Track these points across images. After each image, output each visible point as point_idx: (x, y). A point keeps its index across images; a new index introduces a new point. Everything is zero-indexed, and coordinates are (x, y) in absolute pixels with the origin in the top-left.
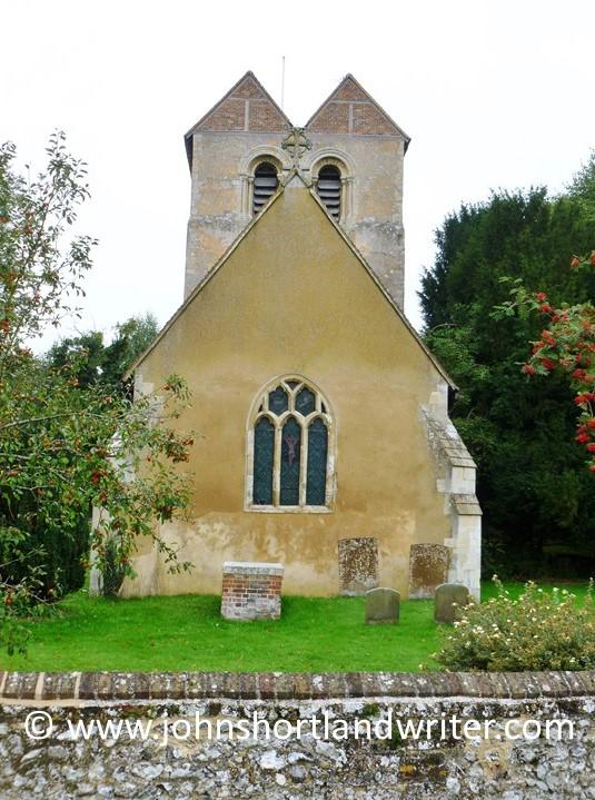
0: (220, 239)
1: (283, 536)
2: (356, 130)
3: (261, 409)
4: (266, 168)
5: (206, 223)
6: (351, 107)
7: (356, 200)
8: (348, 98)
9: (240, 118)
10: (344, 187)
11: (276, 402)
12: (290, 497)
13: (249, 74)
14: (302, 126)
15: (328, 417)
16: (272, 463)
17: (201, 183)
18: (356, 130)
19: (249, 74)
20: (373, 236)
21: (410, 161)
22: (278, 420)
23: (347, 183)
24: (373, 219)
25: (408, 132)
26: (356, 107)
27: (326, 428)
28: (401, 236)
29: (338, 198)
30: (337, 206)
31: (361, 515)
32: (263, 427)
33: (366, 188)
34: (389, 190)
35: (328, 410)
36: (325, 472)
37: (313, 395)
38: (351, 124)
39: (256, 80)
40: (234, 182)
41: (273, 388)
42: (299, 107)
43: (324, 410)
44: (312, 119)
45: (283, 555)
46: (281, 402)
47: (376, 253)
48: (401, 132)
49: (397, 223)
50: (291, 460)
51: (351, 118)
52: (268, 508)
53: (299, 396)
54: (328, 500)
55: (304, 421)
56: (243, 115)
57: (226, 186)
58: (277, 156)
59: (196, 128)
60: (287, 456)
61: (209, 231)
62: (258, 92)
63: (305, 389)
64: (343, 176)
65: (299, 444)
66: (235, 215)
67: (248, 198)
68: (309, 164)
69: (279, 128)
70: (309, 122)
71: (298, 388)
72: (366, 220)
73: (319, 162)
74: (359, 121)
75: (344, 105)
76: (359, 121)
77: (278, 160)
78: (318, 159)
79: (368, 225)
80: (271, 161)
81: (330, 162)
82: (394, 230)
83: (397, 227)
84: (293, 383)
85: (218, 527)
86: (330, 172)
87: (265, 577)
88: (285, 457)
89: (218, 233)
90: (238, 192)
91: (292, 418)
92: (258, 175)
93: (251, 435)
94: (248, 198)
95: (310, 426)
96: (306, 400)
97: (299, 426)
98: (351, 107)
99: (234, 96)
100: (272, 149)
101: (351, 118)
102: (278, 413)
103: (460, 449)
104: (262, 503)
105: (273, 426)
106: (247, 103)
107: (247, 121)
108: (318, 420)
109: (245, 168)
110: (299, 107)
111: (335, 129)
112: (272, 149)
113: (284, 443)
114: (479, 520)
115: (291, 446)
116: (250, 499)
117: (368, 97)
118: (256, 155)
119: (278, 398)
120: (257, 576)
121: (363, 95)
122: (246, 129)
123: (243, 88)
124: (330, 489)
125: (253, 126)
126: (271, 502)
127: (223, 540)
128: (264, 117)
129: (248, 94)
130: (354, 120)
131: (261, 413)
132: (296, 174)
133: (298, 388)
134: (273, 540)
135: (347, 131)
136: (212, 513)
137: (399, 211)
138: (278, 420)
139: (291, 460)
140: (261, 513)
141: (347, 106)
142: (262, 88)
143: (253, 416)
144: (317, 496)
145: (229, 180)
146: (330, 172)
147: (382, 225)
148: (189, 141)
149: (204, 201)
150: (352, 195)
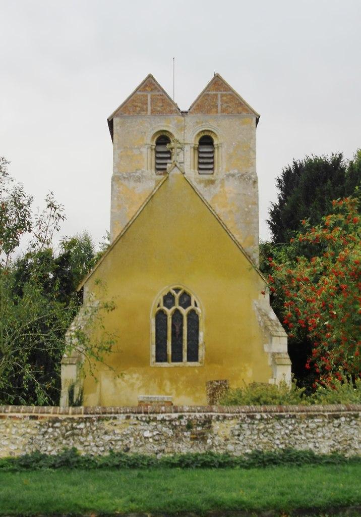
0: (134, 188)
1: (174, 380)
2: (223, 111)
3: (159, 306)
4: (163, 139)
5: (124, 178)
6: (219, 96)
8: (217, 90)
9: (145, 106)
10: (216, 150)
11: (168, 301)
12: (177, 357)
13: (150, 76)
14: (186, 109)
15: (198, 310)
16: (166, 338)
18: (223, 111)
19: (150, 76)
21: (261, 132)
22: (169, 312)
23: (218, 148)
24: (236, 171)
25: (258, 110)
26: (222, 96)
27: (197, 316)
28: (255, 182)
29: (213, 158)
30: (212, 169)
31: (219, 367)
32: (160, 317)
33: (231, 151)
34: (247, 152)
35: (198, 304)
36: (197, 341)
37: (189, 297)
39: (154, 80)
40: (142, 149)
41: (166, 293)
42: (184, 99)
43: (196, 305)
44: (193, 105)
45: (174, 391)
46: (171, 301)
47: (240, 194)
48: (253, 112)
49: (253, 173)
50: (177, 336)
51: (219, 103)
52: (165, 364)
53: (181, 297)
54: (200, 359)
55: (184, 312)
56: (147, 104)
57: (136, 152)
58: (171, 131)
59: (116, 114)
60: (175, 333)
61: (126, 183)
62: (156, 88)
63: (185, 293)
64: (215, 143)
65: (182, 325)
66: (143, 172)
67: (151, 159)
69: (171, 112)
70: (191, 107)
71: (180, 293)
72: (232, 172)
73: (198, 134)
74: (225, 105)
75: (215, 95)
76: (225, 105)
78: (198, 132)
79: (233, 175)
81: (206, 134)
84: (177, 290)
85: (135, 376)
86: (206, 140)
87: (162, 402)
88: (174, 334)
89: (132, 184)
90: (145, 156)
91: (177, 311)
92: (158, 144)
93: (153, 321)
94: (151, 159)
95: (188, 315)
96: (185, 299)
97: (181, 315)
98: (219, 96)
99: (140, 91)
101: (219, 103)
102: (169, 308)
103: (277, 325)
104: (161, 361)
105: (166, 316)
107: (149, 108)
109: (149, 141)
110: (184, 99)
111: (209, 111)
113: (173, 326)
114: (290, 368)
115: (177, 328)
116: (153, 359)
117: (230, 89)
119: (168, 299)
120: (158, 402)
121: (227, 88)
123: (146, 86)
124: (201, 352)
125: (152, 112)
126: (166, 360)
127: (138, 384)
128: (161, 104)
130: (221, 105)
131: (159, 308)
132: (176, 166)
133: (180, 293)
134: (168, 383)
136: (131, 368)
137: (253, 165)
138: (169, 312)
139: (177, 336)
140: (161, 367)
141: (216, 95)
142: (159, 86)
143: (153, 311)
144: (193, 356)
145: (139, 148)
146: (206, 140)
147: (243, 175)
148: (111, 123)
150: (221, 156)
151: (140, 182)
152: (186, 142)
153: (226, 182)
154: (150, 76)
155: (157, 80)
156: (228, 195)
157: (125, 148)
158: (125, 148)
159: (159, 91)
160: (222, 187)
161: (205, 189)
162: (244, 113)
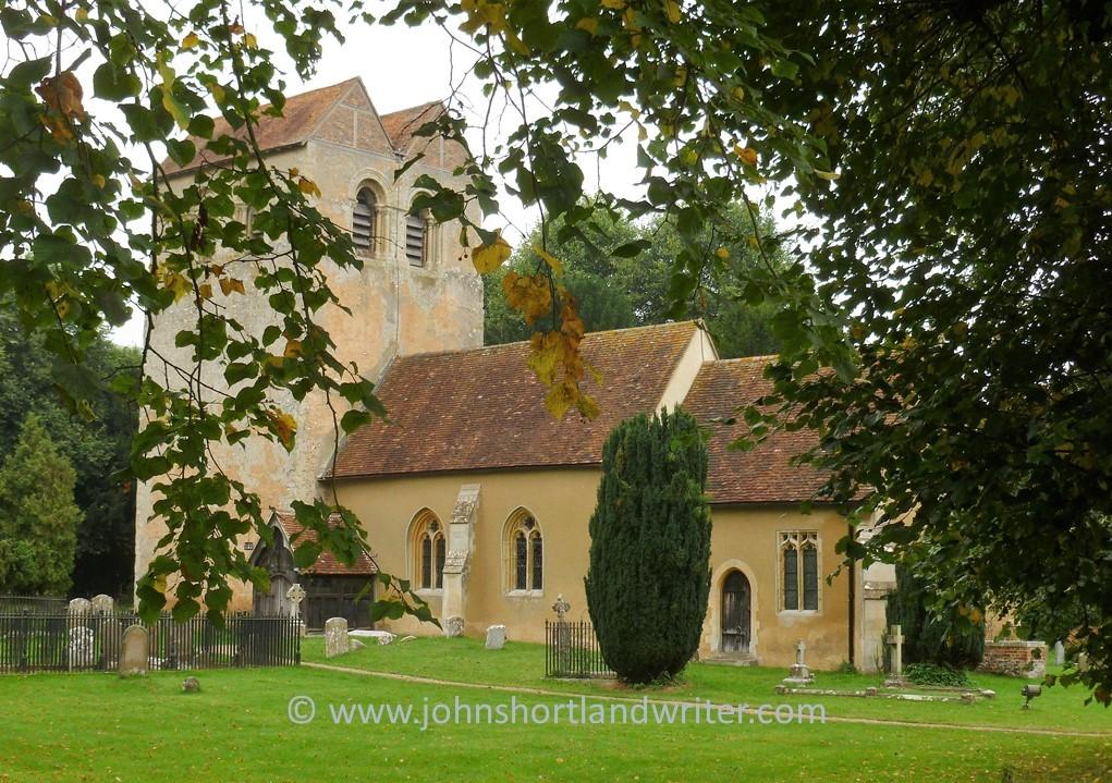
19: (358, 80)
20: (461, 289)
24: (459, 270)
47: (463, 308)
51: (442, 152)
56: (352, 127)
58: (381, 183)
74: (448, 155)
77: (381, 187)
79: (456, 276)
80: (372, 187)
100: (377, 174)
106: (356, 114)
112: (377, 174)
118: (362, 179)
122: (355, 143)
125: (361, 143)
128: (370, 134)
129: (356, 103)
135: (439, 166)
145: (339, 204)
147: (466, 277)
152: (400, 207)
154: (358, 80)
155: (368, 89)
156: (450, 308)
159: (368, 109)
160: (444, 292)
161: (423, 292)
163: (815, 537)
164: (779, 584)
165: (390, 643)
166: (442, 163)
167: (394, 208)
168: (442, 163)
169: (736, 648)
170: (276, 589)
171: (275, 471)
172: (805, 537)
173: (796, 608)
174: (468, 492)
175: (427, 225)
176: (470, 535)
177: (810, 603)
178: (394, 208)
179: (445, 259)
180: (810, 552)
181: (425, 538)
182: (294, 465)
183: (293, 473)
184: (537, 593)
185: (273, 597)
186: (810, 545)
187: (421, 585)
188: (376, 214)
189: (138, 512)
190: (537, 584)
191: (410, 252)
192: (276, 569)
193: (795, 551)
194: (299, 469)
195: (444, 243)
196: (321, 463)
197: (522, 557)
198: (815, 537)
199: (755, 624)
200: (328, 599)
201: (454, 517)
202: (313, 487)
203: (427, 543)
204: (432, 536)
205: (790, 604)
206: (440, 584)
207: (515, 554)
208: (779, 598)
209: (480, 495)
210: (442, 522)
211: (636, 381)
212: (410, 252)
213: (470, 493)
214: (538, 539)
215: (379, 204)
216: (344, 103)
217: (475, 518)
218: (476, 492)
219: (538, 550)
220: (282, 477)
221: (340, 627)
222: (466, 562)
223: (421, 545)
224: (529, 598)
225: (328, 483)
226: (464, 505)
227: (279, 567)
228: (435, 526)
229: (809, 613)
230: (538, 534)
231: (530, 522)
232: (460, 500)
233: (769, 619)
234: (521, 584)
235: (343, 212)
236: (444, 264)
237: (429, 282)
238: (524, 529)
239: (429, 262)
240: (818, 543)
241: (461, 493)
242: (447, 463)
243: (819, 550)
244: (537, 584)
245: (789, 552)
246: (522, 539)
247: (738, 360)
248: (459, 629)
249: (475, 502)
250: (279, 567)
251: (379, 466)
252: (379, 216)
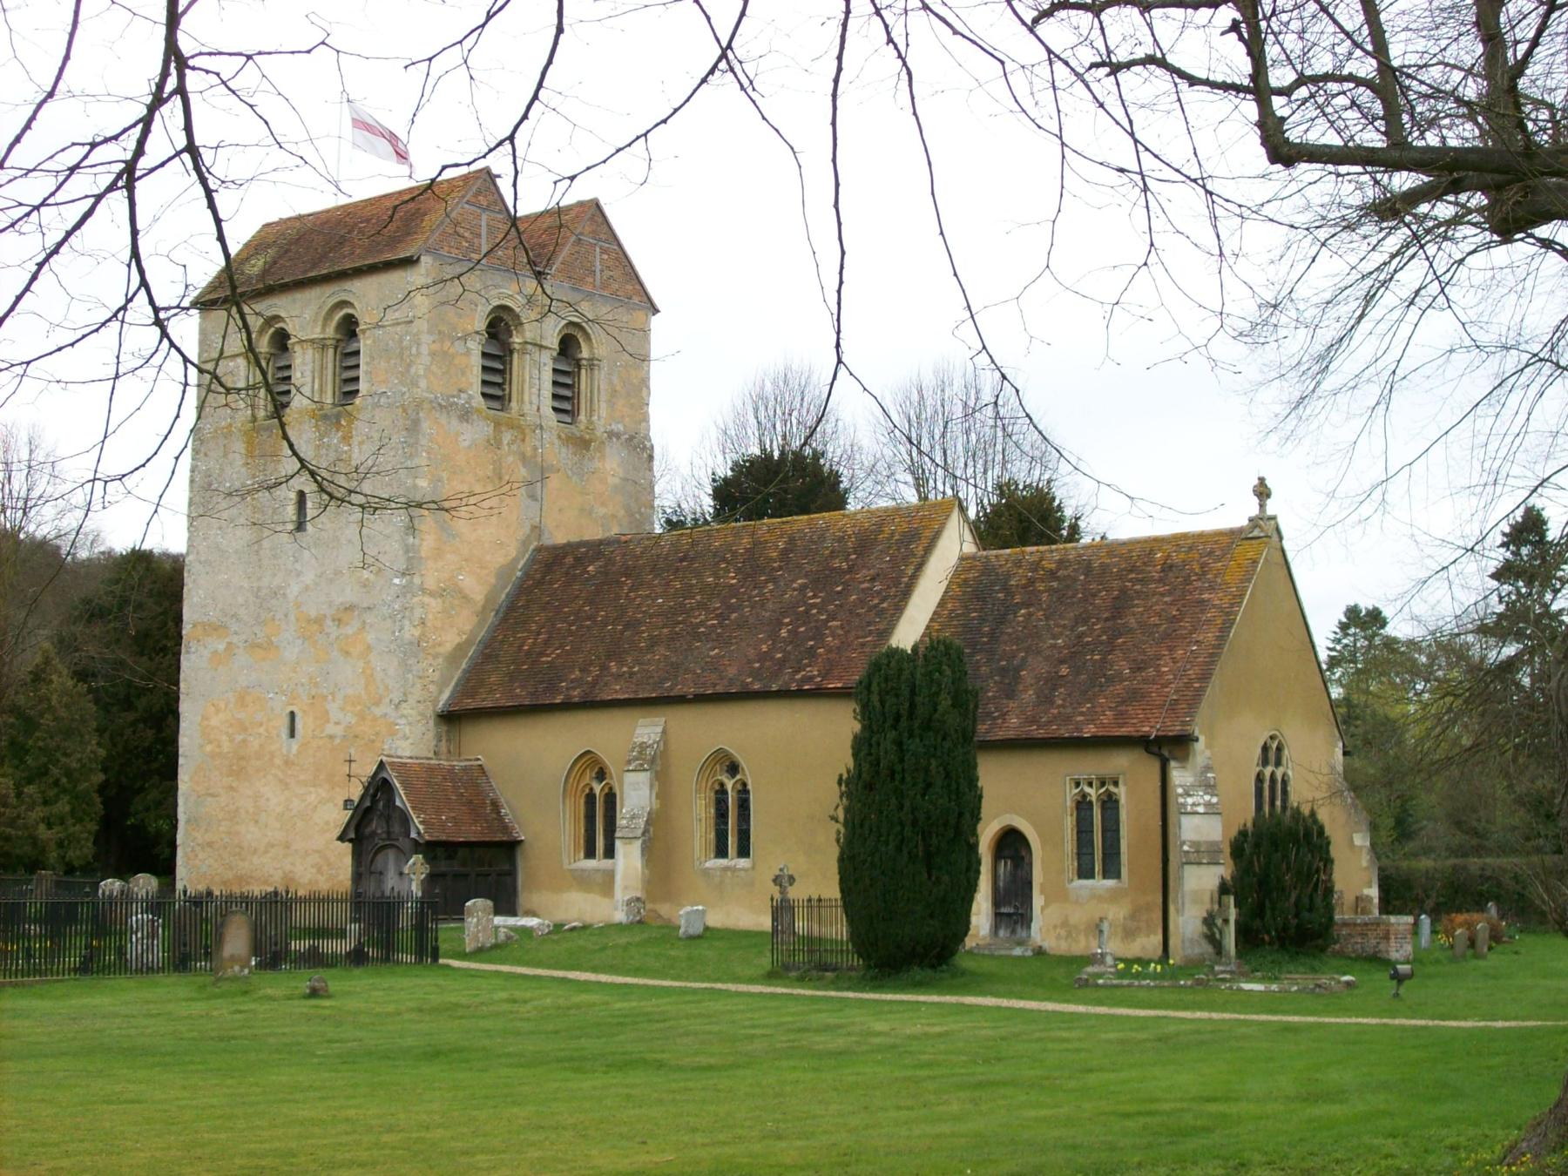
4: (500, 327)
5: (440, 405)
7: (604, 397)
15: (1290, 773)
17: (432, 338)
24: (621, 427)
32: (1259, 779)
38: (598, 273)
51: (598, 267)
56: (479, 236)
64: (585, 353)
66: (471, 397)
68: (551, 334)
74: (607, 273)
76: (607, 273)
79: (618, 435)
81: (570, 331)
82: (645, 447)
83: (648, 445)
86: (568, 346)
106: (484, 217)
108: (1284, 775)
109: (479, 321)
130: (602, 271)
147: (631, 438)
149: (434, 368)
151: (467, 421)
152: (544, 343)
153: (608, 450)
157: (440, 332)
158: (440, 332)
159: (500, 212)
162: (636, 300)
163: (1116, 784)
164: (1070, 845)
165: (549, 933)
166: (598, 283)
167: (535, 345)
168: (598, 283)
169: (1013, 932)
170: (386, 863)
171: (377, 703)
172: (1103, 784)
173: (1092, 877)
174: (647, 729)
175: (579, 367)
176: (651, 786)
177: (1112, 869)
178: (535, 345)
179: (603, 413)
180: (1110, 803)
181: (587, 791)
182: (405, 694)
183: (404, 705)
184: (743, 863)
185: (381, 873)
186: (1110, 795)
187: (582, 855)
188: (511, 352)
189: (181, 761)
190: (744, 851)
191: (557, 405)
192: (384, 836)
193: (1091, 803)
194: (412, 700)
195: (602, 393)
196: (441, 692)
197: (721, 815)
198: (1116, 784)
199: (1038, 900)
200: (456, 876)
201: (629, 762)
202: (432, 723)
203: (590, 799)
204: (597, 788)
205: (1085, 872)
206: (610, 852)
207: (713, 811)
208: (1071, 864)
209: (664, 732)
210: (612, 769)
211: (873, 579)
212: (557, 405)
213: (647, 730)
214: (744, 792)
215: (516, 339)
216: (468, 202)
217: (657, 763)
218: (659, 729)
219: (744, 805)
220: (390, 710)
221: (484, 911)
222: (647, 823)
223: (582, 801)
224: (734, 870)
225: (451, 718)
226: (643, 747)
227: (389, 833)
228: (601, 775)
229: (1111, 883)
230: (744, 785)
231: (733, 769)
232: (638, 740)
233: (1057, 895)
234: (721, 852)
235: (469, 350)
236: (602, 422)
237: (582, 444)
238: (725, 778)
239: (582, 417)
240: (1121, 792)
241: (638, 731)
242: (618, 691)
243: (1123, 801)
244: (744, 851)
245: (1083, 805)
246: (721, 792)
247: (1008, 551)
248: (639, 912)
249: (658, 743)
250: (389, 833)
251: (522, 695)
252: (515, 356)
